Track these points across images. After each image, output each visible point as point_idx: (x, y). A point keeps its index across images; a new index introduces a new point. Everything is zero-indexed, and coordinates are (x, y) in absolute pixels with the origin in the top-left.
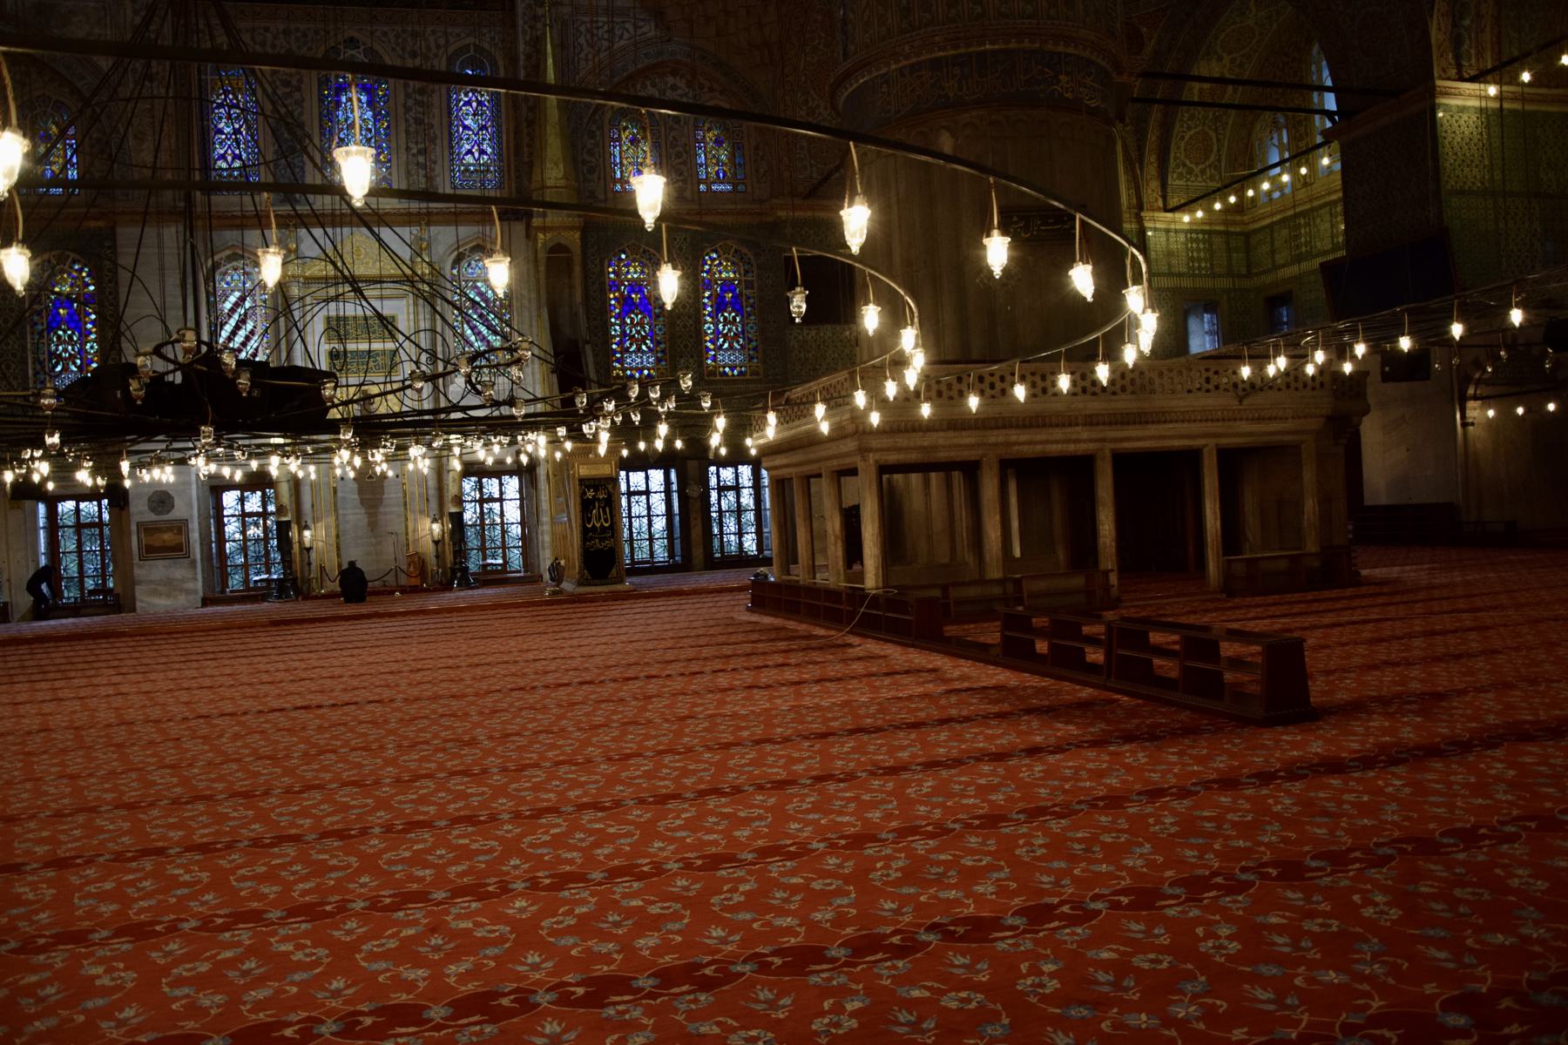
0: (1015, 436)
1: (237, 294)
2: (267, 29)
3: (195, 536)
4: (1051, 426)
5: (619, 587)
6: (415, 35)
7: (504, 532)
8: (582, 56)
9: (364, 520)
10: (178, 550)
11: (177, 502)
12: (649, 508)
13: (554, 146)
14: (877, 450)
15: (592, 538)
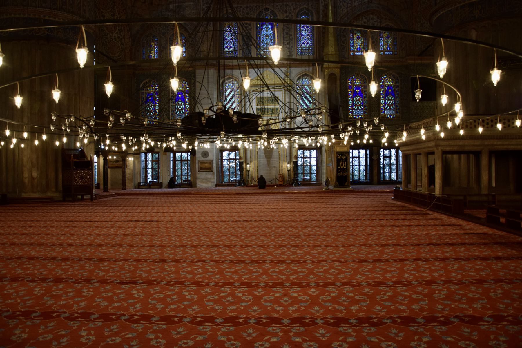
0: (495, 142)
1: (230, 90)
2: (241, 7)
3: (214, 165)
4: (511, 139)
5: (348, 189)
6: (286, 6)
7: (310, 168)
8: (341, 9)
9: (266, 163)
10: (209, 169)
11: (210, 154)
12: (359, 163)
13: (331, 39)
14: (442, 146)
15: (340, 172)
